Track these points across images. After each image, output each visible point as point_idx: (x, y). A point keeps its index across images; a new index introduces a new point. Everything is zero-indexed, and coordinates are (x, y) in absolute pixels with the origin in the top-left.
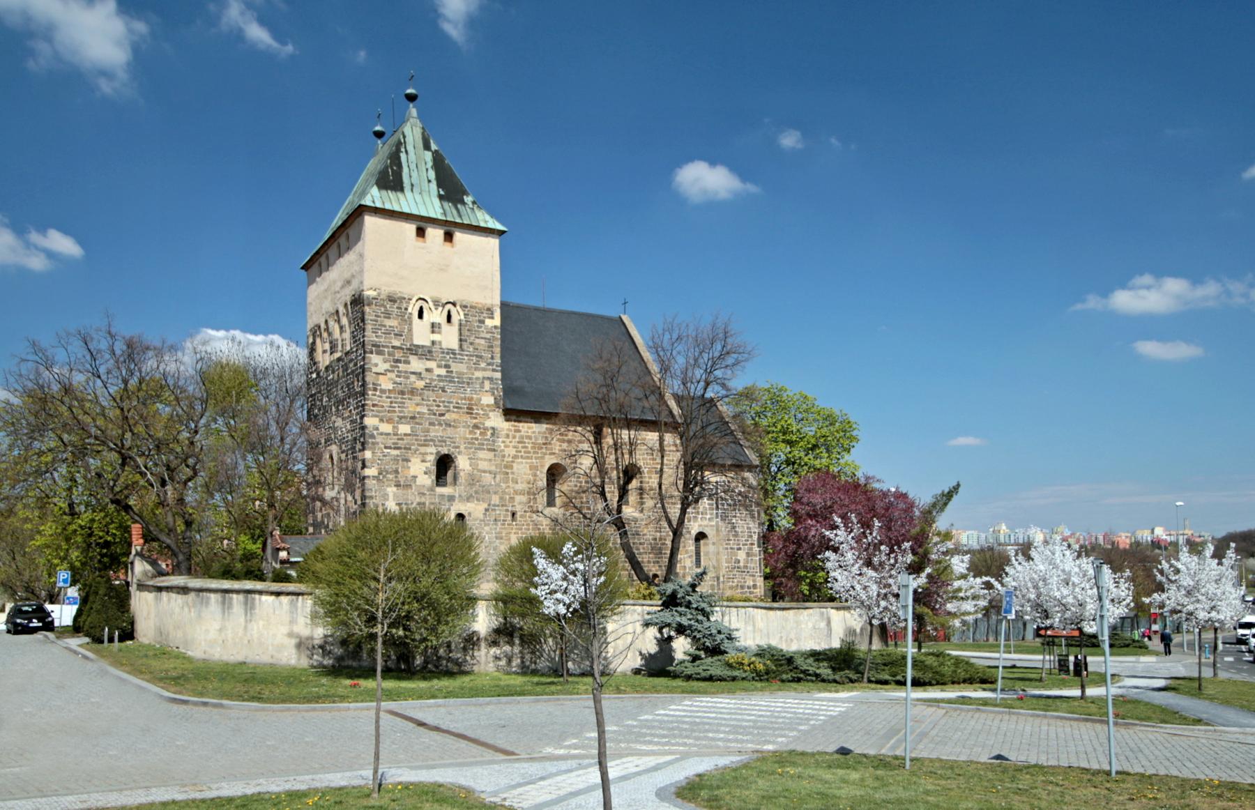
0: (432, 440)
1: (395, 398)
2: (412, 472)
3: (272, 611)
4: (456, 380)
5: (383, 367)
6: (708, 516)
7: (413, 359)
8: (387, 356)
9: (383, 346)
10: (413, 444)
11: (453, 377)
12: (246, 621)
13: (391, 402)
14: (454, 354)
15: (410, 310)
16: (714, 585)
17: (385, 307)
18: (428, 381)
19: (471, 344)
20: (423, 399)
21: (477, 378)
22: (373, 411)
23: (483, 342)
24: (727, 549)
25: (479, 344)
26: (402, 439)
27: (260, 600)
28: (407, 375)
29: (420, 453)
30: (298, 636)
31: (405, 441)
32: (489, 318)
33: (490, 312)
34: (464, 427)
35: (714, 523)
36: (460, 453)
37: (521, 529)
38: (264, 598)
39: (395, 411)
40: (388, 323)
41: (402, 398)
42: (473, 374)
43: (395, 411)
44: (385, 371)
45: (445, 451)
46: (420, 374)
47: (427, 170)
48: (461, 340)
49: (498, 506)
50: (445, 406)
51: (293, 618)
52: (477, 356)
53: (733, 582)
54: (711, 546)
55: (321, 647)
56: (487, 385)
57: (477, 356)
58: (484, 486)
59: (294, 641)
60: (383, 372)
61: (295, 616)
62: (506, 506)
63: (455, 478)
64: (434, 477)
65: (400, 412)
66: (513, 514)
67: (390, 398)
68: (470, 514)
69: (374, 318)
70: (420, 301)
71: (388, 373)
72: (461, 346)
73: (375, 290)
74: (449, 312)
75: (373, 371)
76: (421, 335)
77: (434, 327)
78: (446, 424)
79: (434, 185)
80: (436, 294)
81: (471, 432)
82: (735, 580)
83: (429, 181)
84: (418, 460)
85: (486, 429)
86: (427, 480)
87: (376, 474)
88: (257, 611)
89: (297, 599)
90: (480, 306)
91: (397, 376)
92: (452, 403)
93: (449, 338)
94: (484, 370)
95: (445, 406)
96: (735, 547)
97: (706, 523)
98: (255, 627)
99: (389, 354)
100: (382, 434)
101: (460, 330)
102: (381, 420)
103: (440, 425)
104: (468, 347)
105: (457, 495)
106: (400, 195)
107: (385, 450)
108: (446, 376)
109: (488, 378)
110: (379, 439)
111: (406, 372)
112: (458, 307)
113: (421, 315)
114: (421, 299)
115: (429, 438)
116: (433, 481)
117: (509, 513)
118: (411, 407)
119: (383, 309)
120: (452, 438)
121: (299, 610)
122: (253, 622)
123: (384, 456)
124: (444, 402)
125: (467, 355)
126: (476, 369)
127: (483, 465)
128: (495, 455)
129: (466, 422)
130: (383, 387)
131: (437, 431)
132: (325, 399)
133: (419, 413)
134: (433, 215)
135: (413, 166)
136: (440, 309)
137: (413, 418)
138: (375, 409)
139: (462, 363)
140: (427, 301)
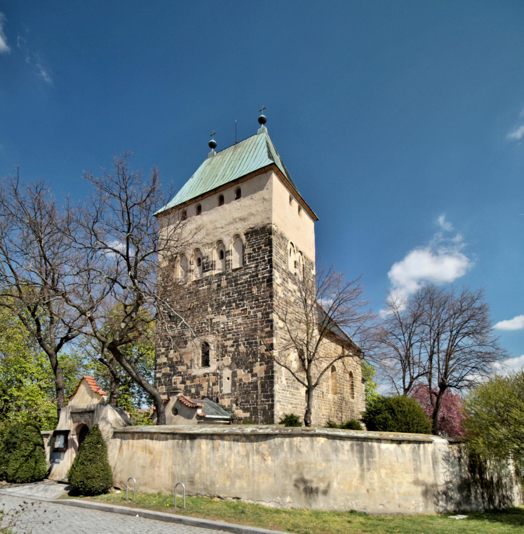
3: (395, 459)
12: (362, 470)
27: (379, 447)
30: (424, 484)
38: (384, 446)
51: (417, 466)
55: (445, 493)
59: (420, 489)
61: (418, 464)
88: (377, 459)
89: (419, 447)
98: (375, 476)
121: (422, 458)
122: (372, 471)
140: (293, 246)
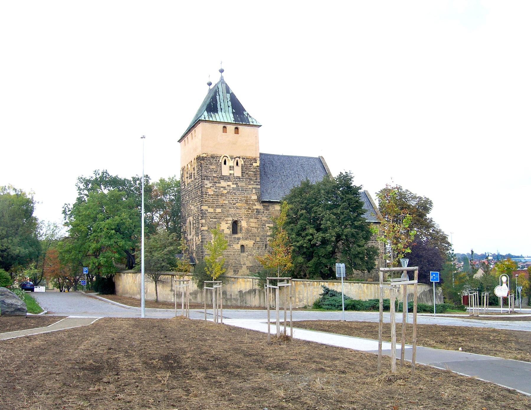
0: (230, 215)
1: (214, 198)
2: (222, 228)
4: (240, 189)
5: (209, 185)
7: (222, 181)
8: (211, 181)
9: (209, 177)
10: (223, 217)
11: (239, 188)
13: (213, 200)
14: (240, 179)
15: (220, 161)
17: (210, 160)
18: (228, 190)
19: (247, 174)
20: (226, 198)
21: (250, 188)
22: (205, 203)
23: (252, 173)
25: (250, 174)
26: (218, 215)
28: (219, 188)
29: (225, 220)
31: (219, 215)
32: (255, 163)
33: (255, 160)
34: (244, 209)
36: (242, 220)
39: (215, 203)
40: (211, 167)
41: (217, 198)
42: (248, 187)
43: (215, 203)
44: (210, 187)
45: (236, 219)
46: (225, 187)
47: (228, 102)
48: (242, 173)
49: (259, 242)
50: (236, 201)
52: (249, 179)
56: (254, 191)
57: (249, 179)
58: (253, 234)
60: (209, 187)
62: (263, 242)
63: (241, 230)
64: (231, 230)
65: (217, 203)
67: (213, 198)
68: (247, 245)
69: (205, 165)
70: (225, 157)
71: (211, 188)
72: (242, 175)
73: (206, 154)
74: (237, 161)
75: (205, 187)
76: (226, 171)
77: (231, 168)
78: (236, 208)
79: (230, 109)
80: (231, 154)
81: (247, 211)
83: (229, 107)
84: (225, 223)
85: (254, 209)
86: (228, 231)
87: (207, 229)
90: (251, 158)
91: (215, 189)
92: (239, 199)
93: (238, 172)
94: (253, 184)
95: (236, 201)
99: (212, 180)
100: (209, 213)
101: (242, 168)
102: (209, 207)
103: (234, 208)
104: (245, 175)
105: (241, 238)
106: (216, 114)
107: (211, 219)
108: (236, 188)
109: (255, 188)
110: (208, 215)
111: (219, 187)
112: (241, 159)
113: (225, 163)
114: (225, 156)
115: (229, 214)
116: (231, 231)
117: (264, 245)
118: (221, 201)
119: (209, 161)
120: (239, 214)
123: (210, 222)
124: (235, 199)
125: (245, 179)
126: (249, 184)
127: (253, 225)
128: (258, 220)
129: (245, 207)
130: (209, 193)
131: (232, 211)
132: (187, 197)
133: (224, 204)
134: (230, 121)
135: (222, 101)
136: (233, 160)
137: (221, 206)
138: (206, 202)
139: (243, 182)
140: (228, 158)
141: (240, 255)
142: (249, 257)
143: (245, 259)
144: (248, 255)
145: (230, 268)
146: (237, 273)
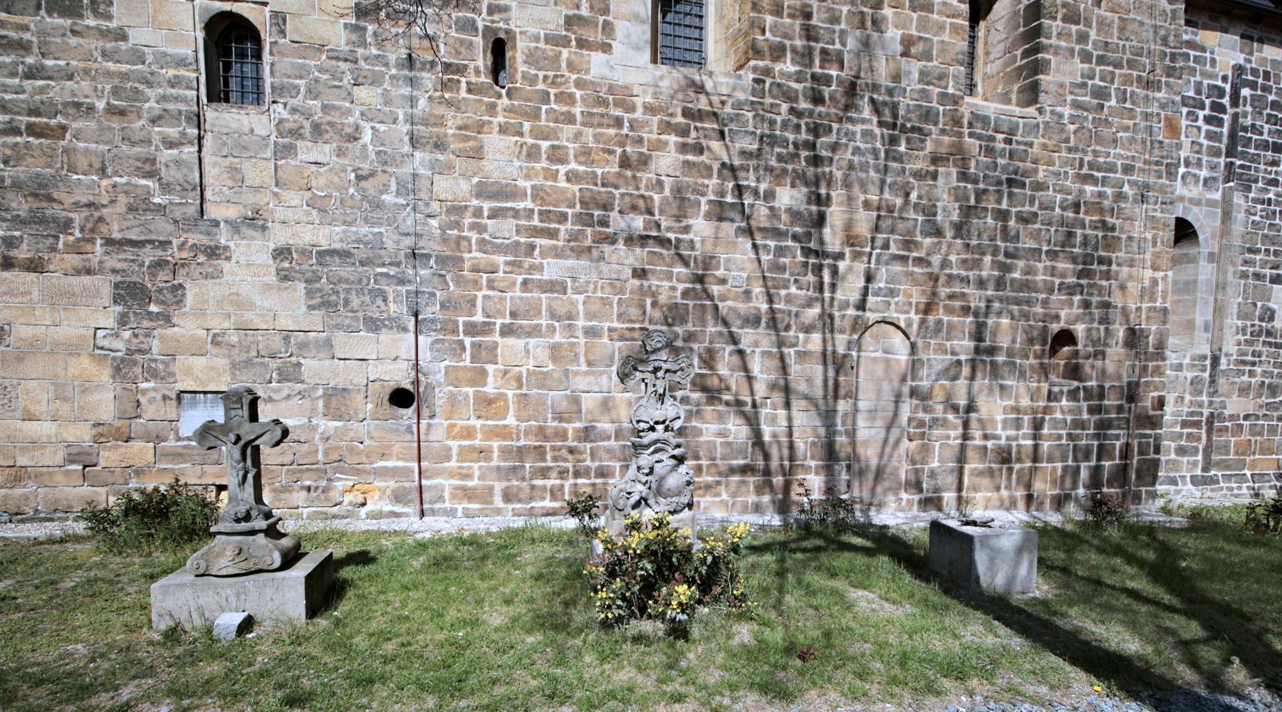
6: (1204, 173)
16: (1201, 380)
24: (1244, 275)
35: (1217, 196)
37: (535, 115)
53: (1251, 374)
54: (1203, 263)
66: (499, 49)
82: (1258, 370)
96: (1267, 271)
97: (1195, 191)
117: (479, 41)
141: (198, 120)
142: (308, 151)
143: (258, 171)
144: (296, 133)
145: (74, 260)
146: (167, 319)
